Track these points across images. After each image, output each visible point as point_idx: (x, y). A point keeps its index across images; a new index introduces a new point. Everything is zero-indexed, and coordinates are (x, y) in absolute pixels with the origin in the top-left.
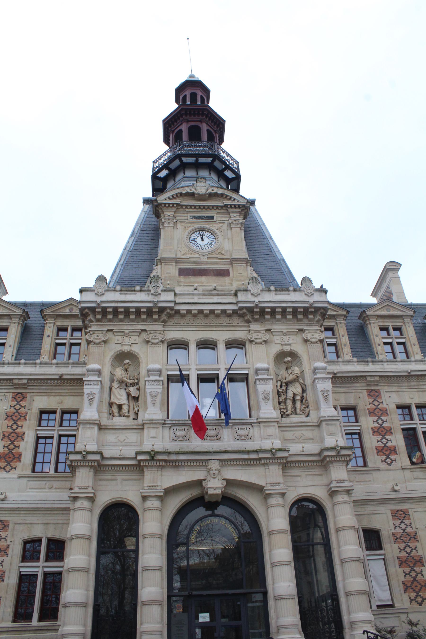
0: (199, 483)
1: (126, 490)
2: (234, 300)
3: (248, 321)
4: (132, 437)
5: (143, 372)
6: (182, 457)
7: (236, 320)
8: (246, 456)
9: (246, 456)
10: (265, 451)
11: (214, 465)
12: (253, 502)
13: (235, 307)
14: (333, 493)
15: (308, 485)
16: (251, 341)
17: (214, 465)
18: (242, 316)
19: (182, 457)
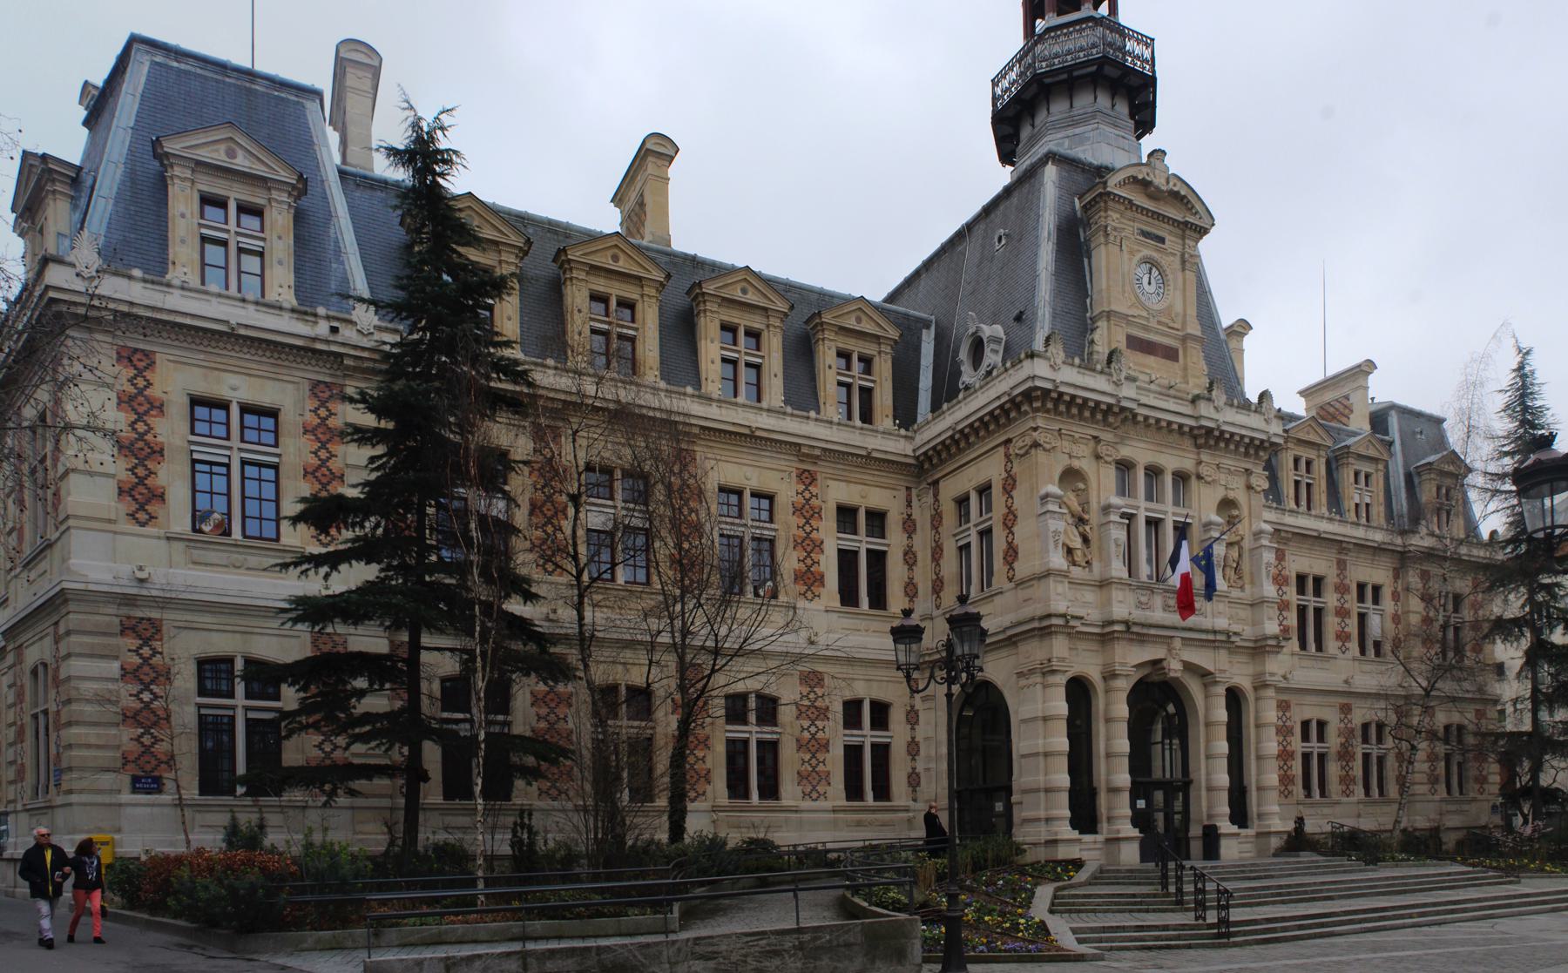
0: (1156, 663)
1: (1088, 665)
2: (1187, 410)
3: (1198, 447)
4: (1090, 596)
5: (1094, 506)
6: (1153, 631)
7: (1188, 443)
8: (1204, 636)
9: (1204, 636)
10: (1220, 632)
11: (1177, 643)
12: (1194, 687)
13: (1192, 423)
14: (1260, 685)
15: (1239, 674)
16: (1199, 477)
17: (1177, 643)
18: (1195, 437)
19: (1153, 631)
